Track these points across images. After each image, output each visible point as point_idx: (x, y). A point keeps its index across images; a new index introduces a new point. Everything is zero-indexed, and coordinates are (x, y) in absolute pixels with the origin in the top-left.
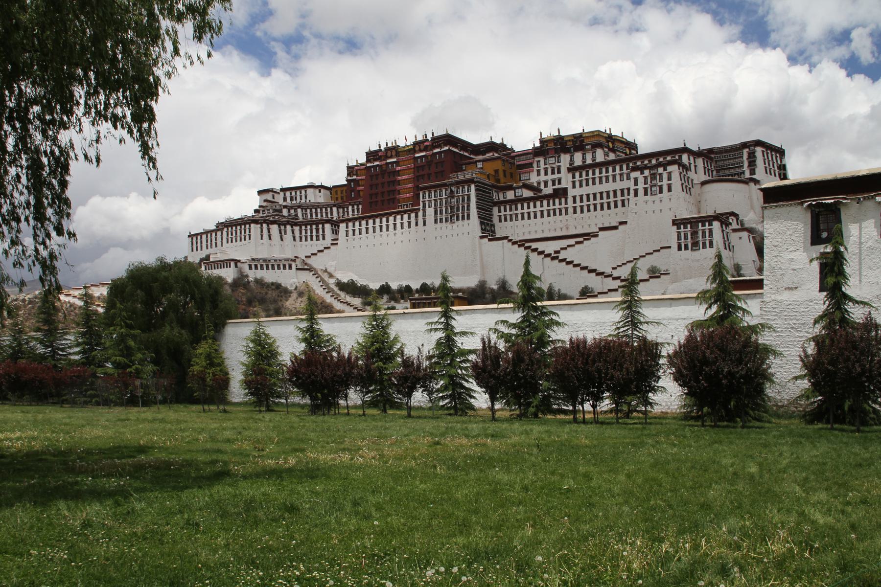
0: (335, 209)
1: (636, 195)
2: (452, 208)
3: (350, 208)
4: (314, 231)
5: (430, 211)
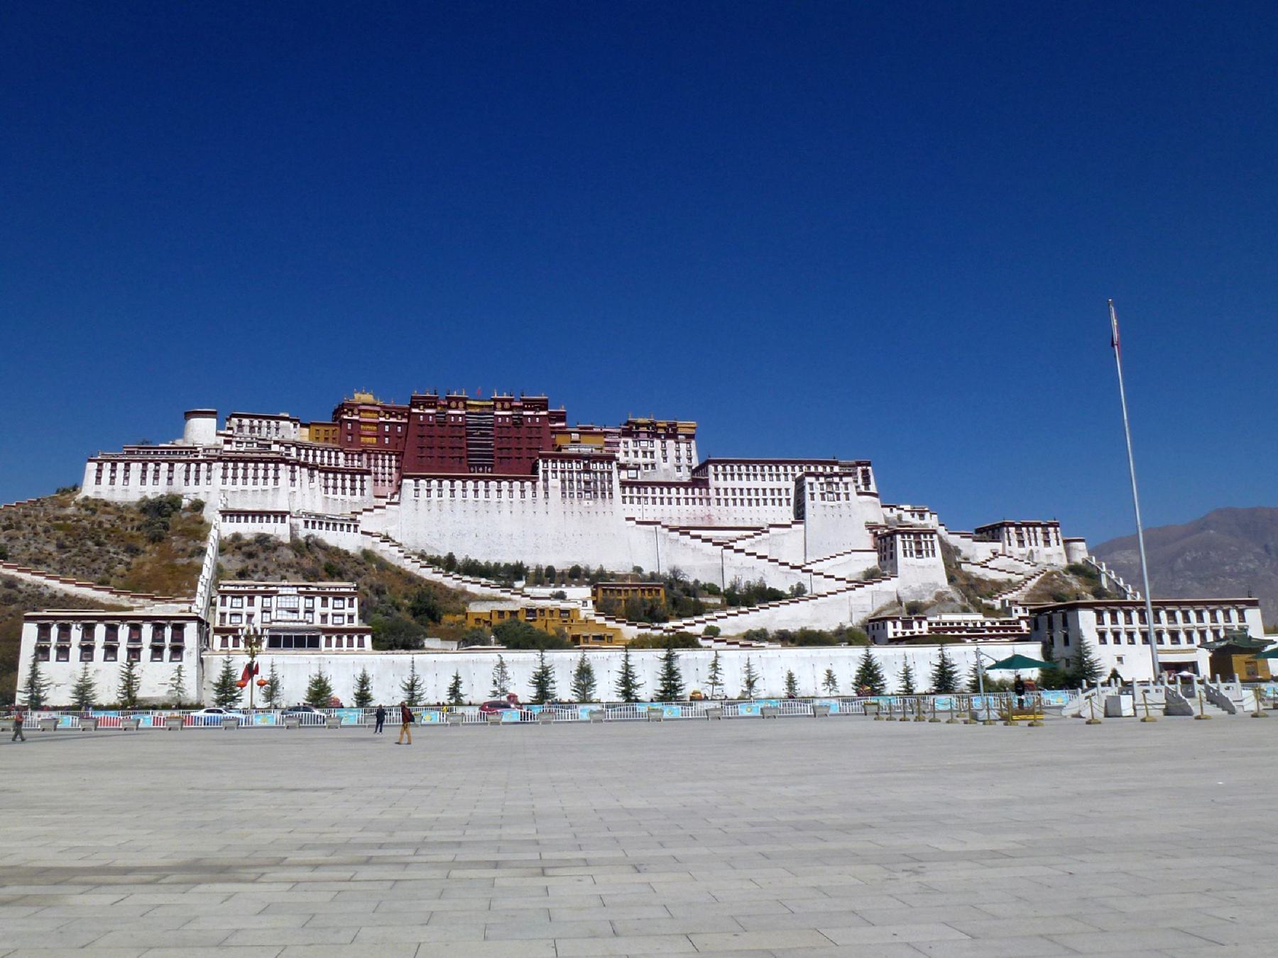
0: (341, 455)
1: (813, 499)
2: (587, 483)
3: (365, 457)
4: (348, 483)
5: (555, 483)
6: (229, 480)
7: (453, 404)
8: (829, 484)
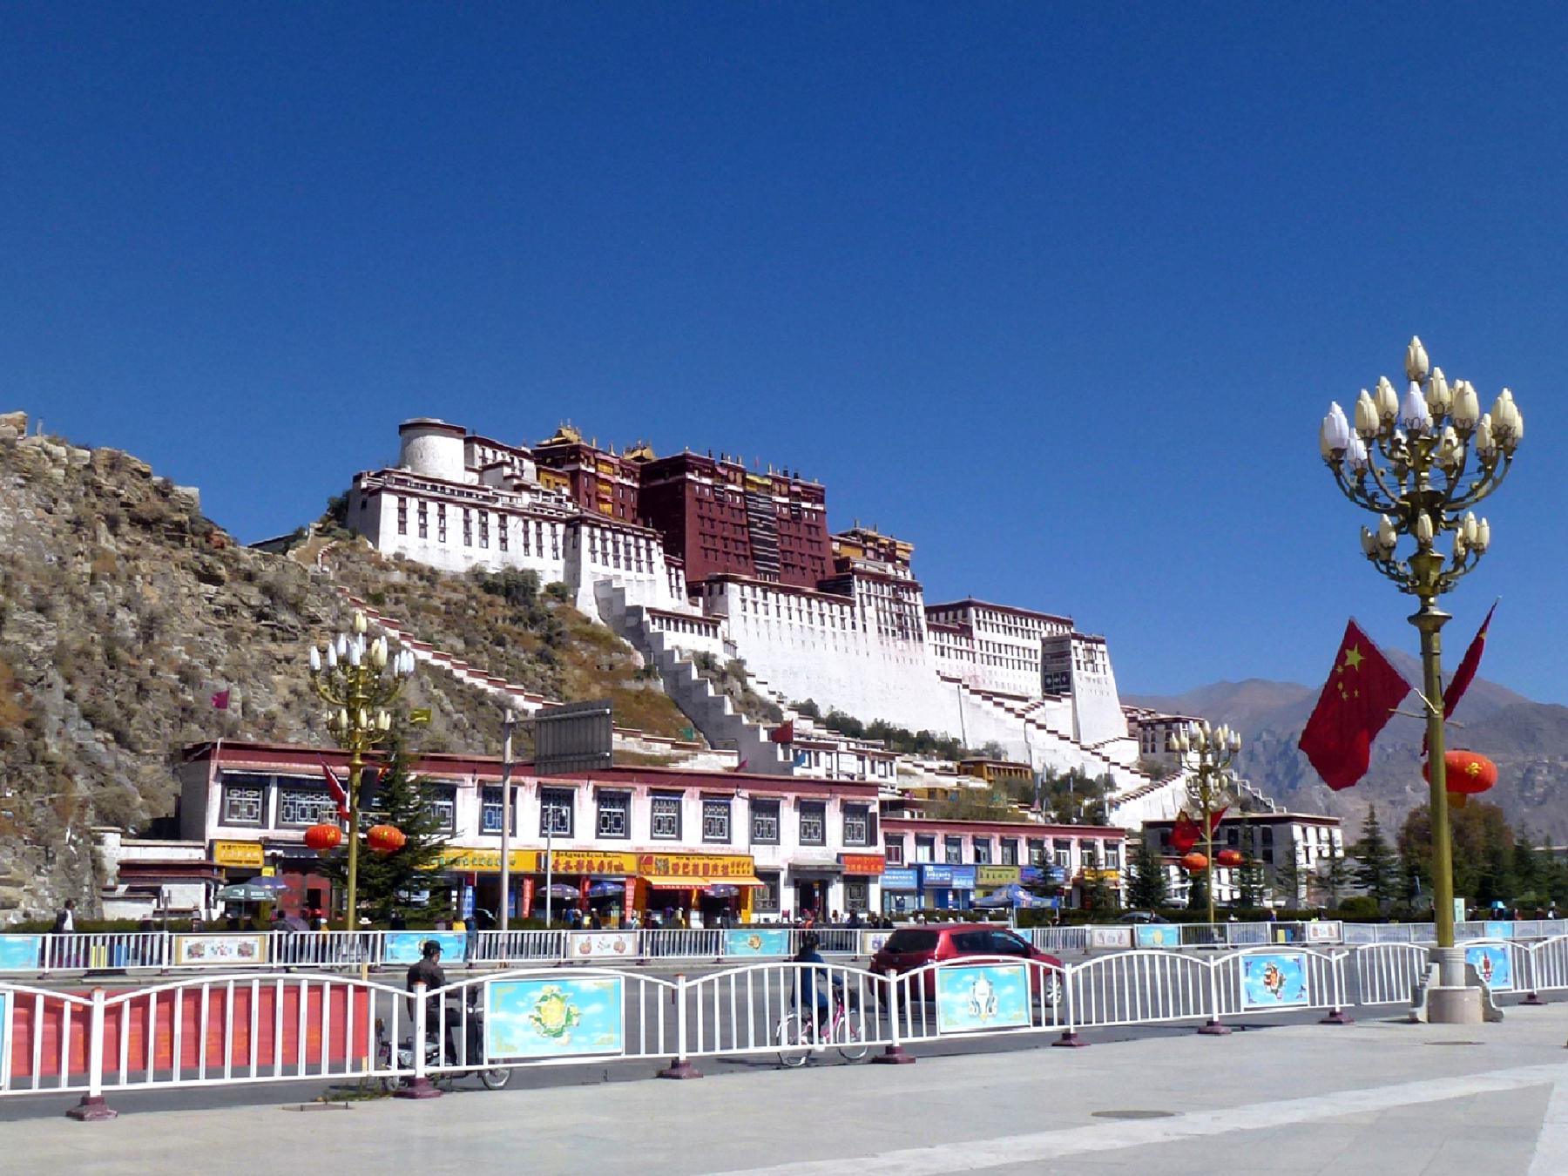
5: (870, 611)
6: (599, 556)
7: (732, 477)
8: (1090, 651)
